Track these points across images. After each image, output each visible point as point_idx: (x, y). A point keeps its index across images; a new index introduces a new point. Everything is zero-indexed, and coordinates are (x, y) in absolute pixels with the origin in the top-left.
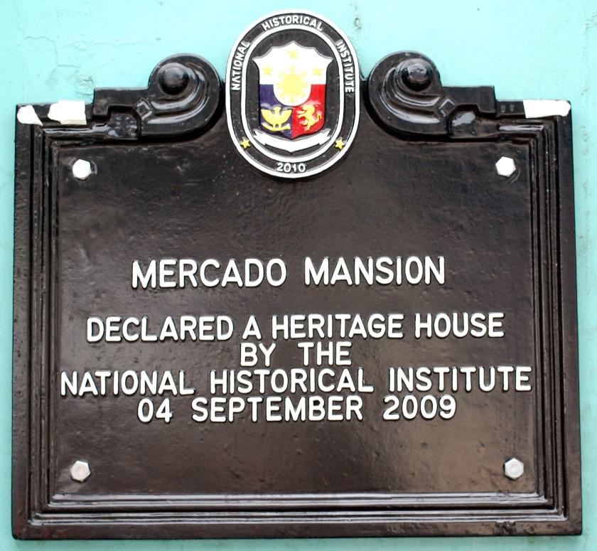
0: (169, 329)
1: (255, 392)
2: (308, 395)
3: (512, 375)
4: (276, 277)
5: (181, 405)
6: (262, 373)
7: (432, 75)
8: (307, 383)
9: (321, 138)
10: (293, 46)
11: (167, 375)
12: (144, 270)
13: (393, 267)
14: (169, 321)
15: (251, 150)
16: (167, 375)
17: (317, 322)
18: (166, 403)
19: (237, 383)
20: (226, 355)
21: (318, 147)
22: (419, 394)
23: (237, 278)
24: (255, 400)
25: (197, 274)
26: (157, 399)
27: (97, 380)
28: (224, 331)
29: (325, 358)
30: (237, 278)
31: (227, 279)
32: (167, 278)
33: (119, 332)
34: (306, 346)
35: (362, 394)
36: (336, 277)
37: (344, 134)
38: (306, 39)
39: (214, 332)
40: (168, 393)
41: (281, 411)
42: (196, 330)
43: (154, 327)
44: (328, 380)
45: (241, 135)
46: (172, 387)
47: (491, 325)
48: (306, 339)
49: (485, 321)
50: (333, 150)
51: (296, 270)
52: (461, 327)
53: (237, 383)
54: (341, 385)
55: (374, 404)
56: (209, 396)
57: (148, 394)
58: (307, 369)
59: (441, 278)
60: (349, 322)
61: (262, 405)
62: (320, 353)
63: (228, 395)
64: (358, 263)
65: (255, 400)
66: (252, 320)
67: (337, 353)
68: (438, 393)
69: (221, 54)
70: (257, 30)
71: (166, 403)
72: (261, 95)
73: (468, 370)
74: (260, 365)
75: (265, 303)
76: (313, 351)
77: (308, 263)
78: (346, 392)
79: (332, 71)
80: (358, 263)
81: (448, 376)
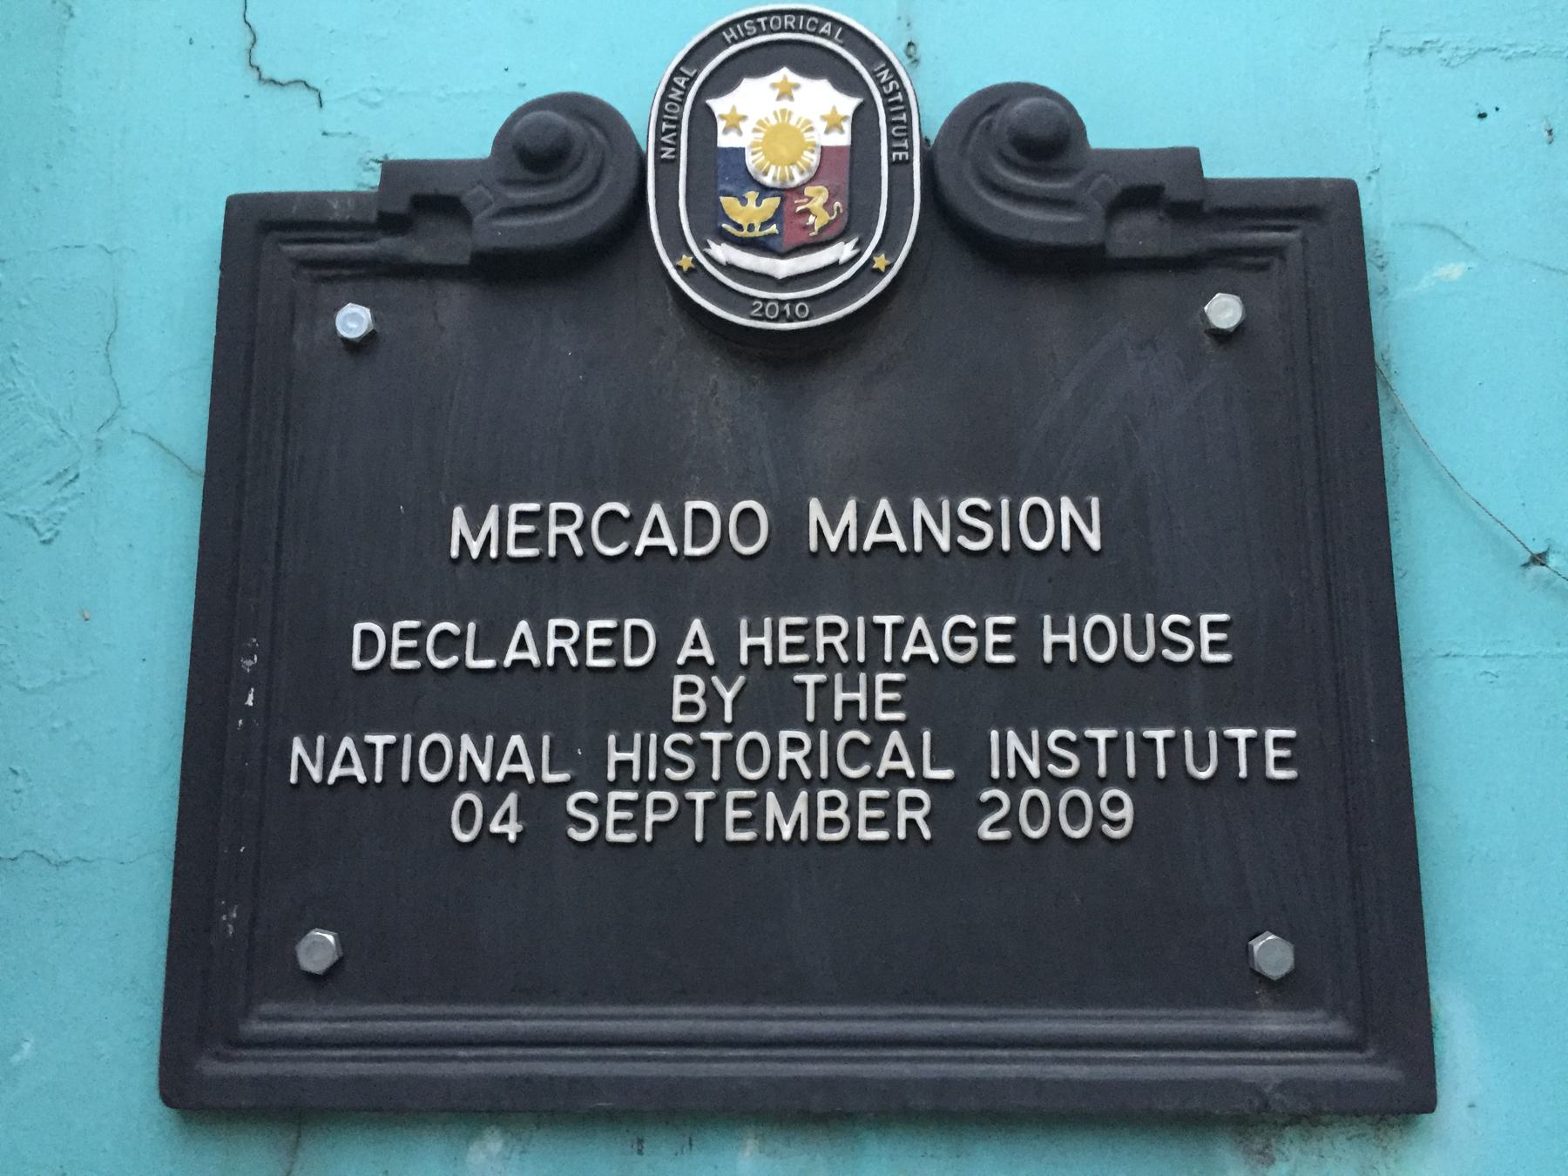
0: (522, 646)
2: (814, 784)
3: (1255, 745)
4: (748, 535)
5: (541, 804)
6: (716, 737)
8: (812, 759)
10: (784, 74)
11: (516, 741)
12: (475, 523)
13: (992, 516)
14: (523, 627)
15: (695, 273)
16: (516, 741)
17: (832, 630)
18: (511, 800)
20: (636, 699)
21: (835, 268)
22: (1055, 785)
23: (667, 540)
24: (700, 797)
25: (583, 532)
26: (493, 792)
28: (638, 648)
29: (850, 706)
30: (667, 540)
31: (645, 541)
32: (521, 539)
34: (811, 680)
35: (930, 784)
37: (889, 244)
38: (813, 62)
39: (613, 651)
40: (515, 779)
41: (757, 821)
43: (492, 642)
45: (677, 246)
46: (526, 767)
49: (1192, 631)
50: (869, 273)
51: (790, 523)
52: (1139, 644)
54: (886, 764)
55: (956, 805)
56: (604, 787)
59: (1094, 540)
60: (901, 630)
61: (714, 808)
62: (840, 696)
63: (644, 785)
64: (920, 509)
65: (700, 797)
66: (697, 626)
67: (878, 695)
68: (1097, 786)
70: (714, 41)
71: (511, 800)
72: (721, 171)
73: (1160, 735)
74: (713, 718)
75: (726, 590)
77: (816, 510)
78: (896, 778)
79: (863, 119)
80: (920, 509)
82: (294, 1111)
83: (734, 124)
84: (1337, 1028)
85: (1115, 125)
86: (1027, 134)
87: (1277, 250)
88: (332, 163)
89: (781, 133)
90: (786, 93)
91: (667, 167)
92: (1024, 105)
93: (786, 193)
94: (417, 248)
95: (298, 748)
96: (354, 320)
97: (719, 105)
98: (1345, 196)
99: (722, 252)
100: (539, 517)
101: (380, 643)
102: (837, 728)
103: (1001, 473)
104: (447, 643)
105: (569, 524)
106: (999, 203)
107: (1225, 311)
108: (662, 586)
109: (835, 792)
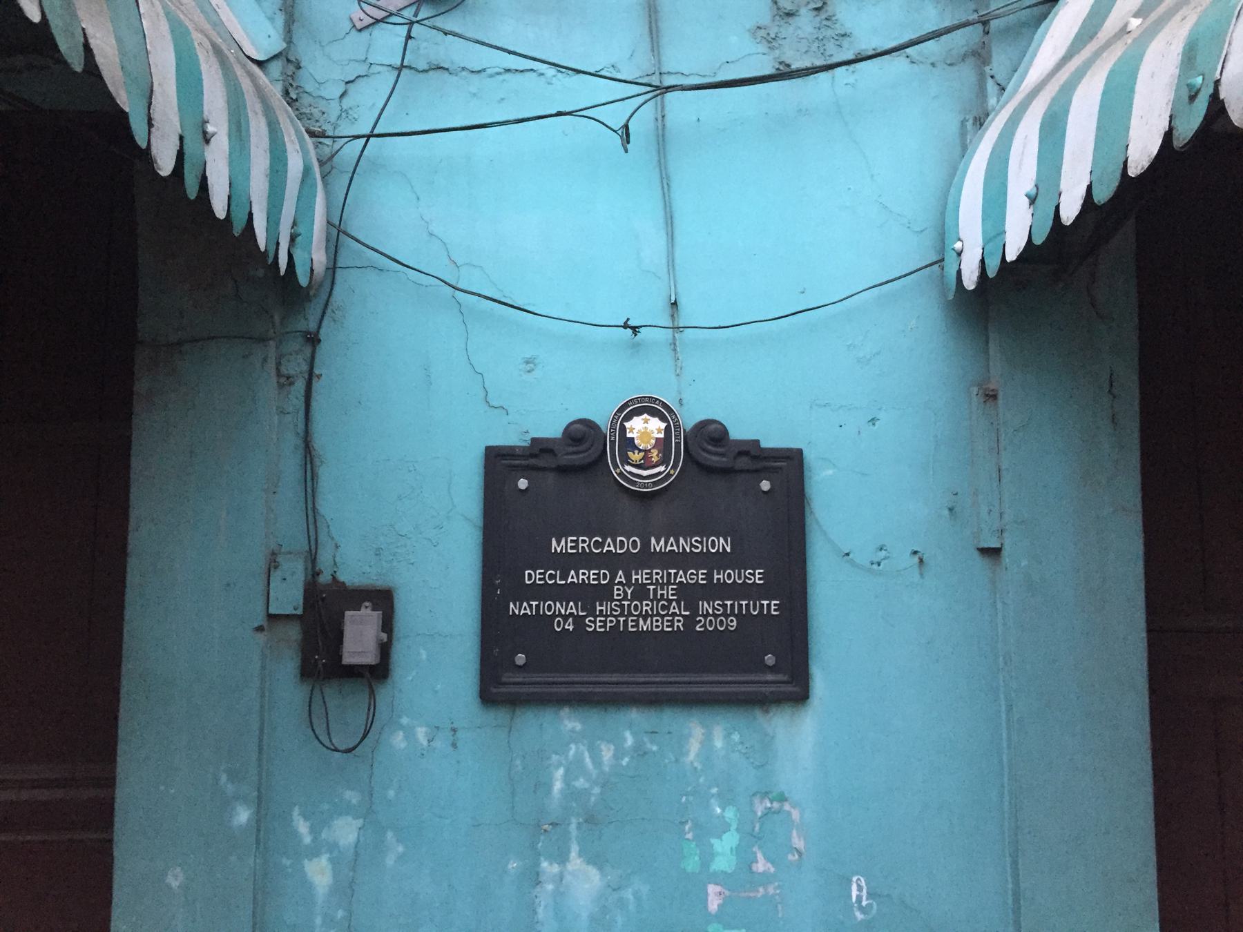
1: (622, 615)
2: (652, 616)
3: (769, 605)
4: (635, 548)
5: (579, 621)
6: (626, 603)
7: (724, 432)
8: (652, 609)
9: (662, 468)
10: (645, 416)
11: (571, 604)
12: (559, 543)
13: (701, 543)
14: (572, 572)
15: (621, 474)
16: (571, 604)
17: (658, 575)
19: (612, 609)
20: (604, 593)
21: (660, 473)
23: (612, 548)
24: (622, 619)
25: (589, 546)
26: (566, 618)
27: (531, 606)
28: (605, 579)
29: (662, 595)
30: (612, 548)
31: (606, 549)
32: (572, 548)
33: (544, 579)
34: (652, 587)
35: (683, 616)
36: (669, 548)
37: (674, 467)
38: (654, 413)
39: (598, 579)
41: (637, 626)
42: (588, 578)
44: (663, 607)
45: (616, 466)
46: (574, 611)
47: (757, 576)
48: (651, 584)
49: (754, 575)
50: (669, 475)
51: (646, 544)
52: (740, 578)
53: (612, 609)
54: (672, 610)
55: (690, 621)
56: (596, 617)
57: (560, 615)
58: (652, 601)
59: (728, 550)
62: (660, 592)
63: (607, 616)
65: (622, 619)
66: (620, 573)
67: (670, 592)
68: (727, 616)
69: (602, 415)
72: (629, 444)
73: (744, 603)
74: (625, 598)
75: (628, 562)
76: (655, 591)
77: (653, 541)
78: (674, 614)
79: (668, 429)
81: (732, 605)
82: (515, 702)
83: (632, 430)
84: (785, 678)
85: (738, 432)
86: (710, 434)
87: (781, 468)
88: (511, 436)
89: (645, 434)
90: (646, 421)
91: (612, 443)
92: (713, 426)
93: (646, 451)
94: (540, 463)
95: (512, 605)
96: (523, 484)
97: (627, 425)
98: (800, 452)
99: (628, 468)
100: (576, 541)
101: (532, 576)
102: (659, 601)
103: (704, 531)
104: (552, 577)
105: (585, 543)
106: (705, 455)
107: (765, 485)
108: (610, 562)
109: (659, 618)
